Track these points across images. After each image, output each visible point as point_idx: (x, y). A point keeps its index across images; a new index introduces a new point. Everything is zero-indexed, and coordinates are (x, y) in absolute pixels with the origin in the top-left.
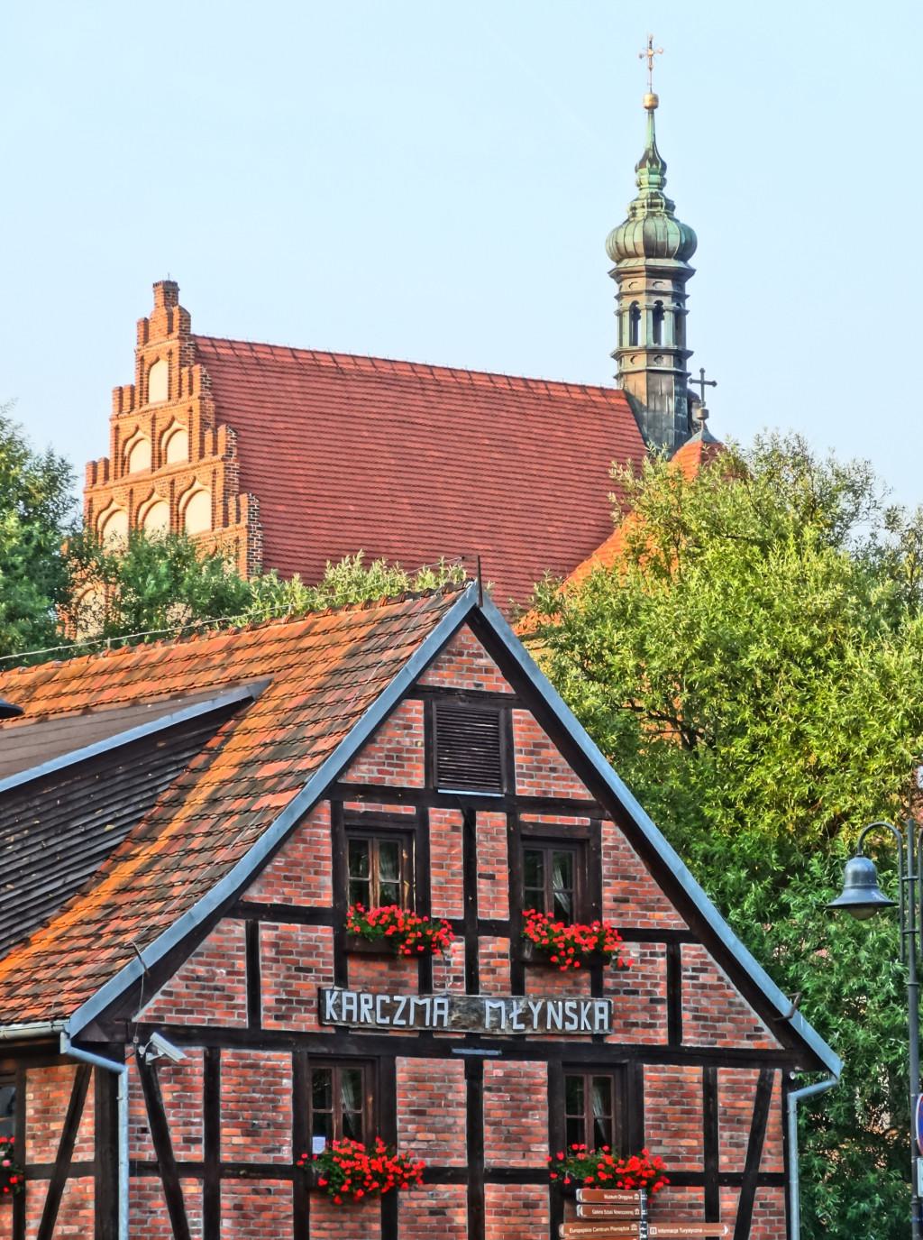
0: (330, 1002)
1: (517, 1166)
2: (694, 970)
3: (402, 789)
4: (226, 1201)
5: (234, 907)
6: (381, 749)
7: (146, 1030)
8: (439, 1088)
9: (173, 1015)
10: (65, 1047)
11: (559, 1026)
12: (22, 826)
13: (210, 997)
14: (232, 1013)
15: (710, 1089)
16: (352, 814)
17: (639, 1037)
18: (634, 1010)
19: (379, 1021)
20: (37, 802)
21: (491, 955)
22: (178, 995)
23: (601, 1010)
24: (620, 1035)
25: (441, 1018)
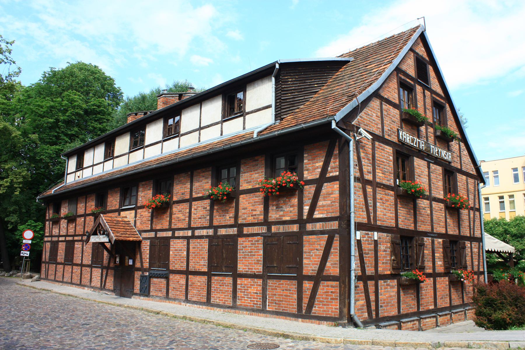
0: (401, 134)
4: (378, 196)
5: (376, 94)
10: (334, 126)
12: (293, 77)
13: (372, 123)
22: (364, 119)
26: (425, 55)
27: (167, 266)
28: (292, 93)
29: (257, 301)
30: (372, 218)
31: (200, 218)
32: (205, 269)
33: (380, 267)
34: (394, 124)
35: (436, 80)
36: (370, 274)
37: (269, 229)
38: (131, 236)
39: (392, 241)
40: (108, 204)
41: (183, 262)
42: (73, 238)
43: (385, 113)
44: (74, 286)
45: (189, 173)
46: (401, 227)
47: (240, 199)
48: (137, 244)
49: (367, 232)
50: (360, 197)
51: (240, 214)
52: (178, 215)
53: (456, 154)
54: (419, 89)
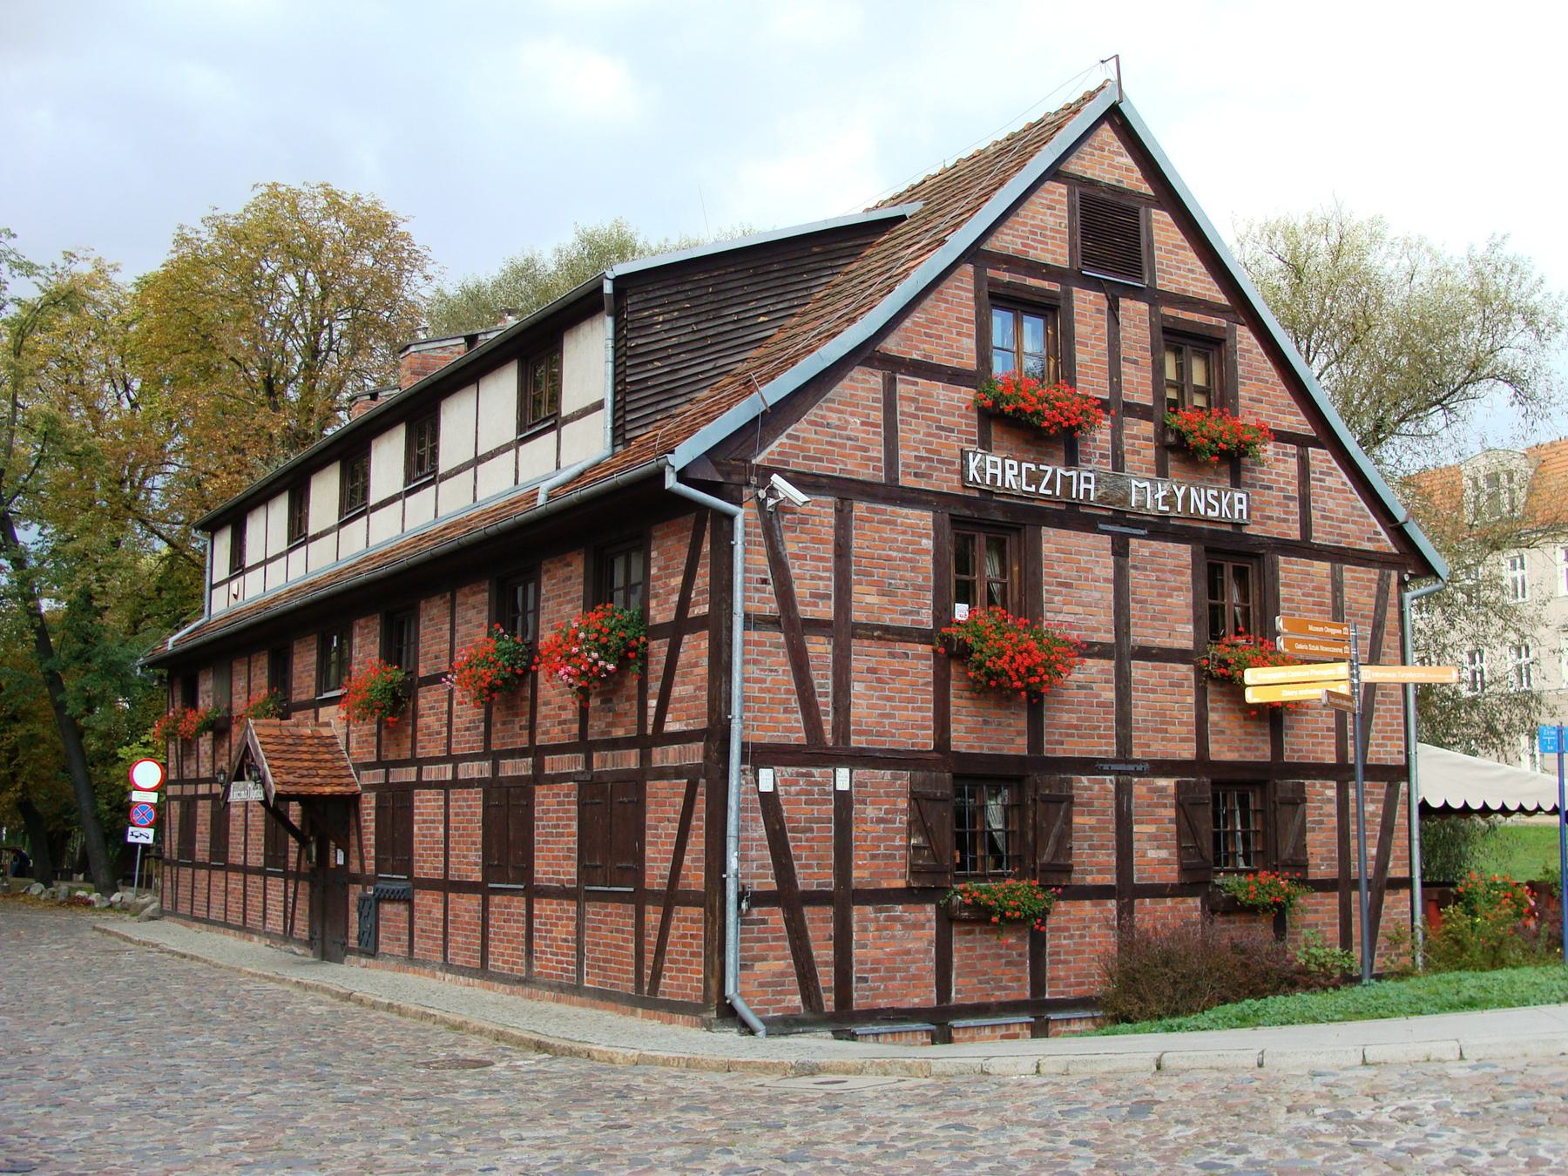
0: (972, 465)
1: (1163, 645)
2: (1321, 473)
3: (1046, 266)
4: (858, 663)
5: (865, 354)
6: (1025, 224)
7: (766, 472)
8: (1086, 562)
9: (800, 460)
10: (671, 482)
11: (1202, 513)
14: (867, 466)
15: (1337, 587)
16: (993, 283)
17: (1274, 530)
18: (1269, 503)
19: (1025, 488)
20: (687, 287)
21: (1135, 437)
23: (1240, 501)
24: (1257, 527)
25: (1087, 491)
26: (1132, 178)
27: (406, 866)
28: (669, 357)
29: (567, 963)
30: (828, 728)
31: (467, 729)
32: (477, 876)
33: (859, 867)
34: (947, 438)
35: (1191, 257)
36: (815, 888)
37: (588, 762)
38: (329, 780)
39: (912, 792)
41: (436, 856)
42: (387, 775)
43: (902, 407)
44: (231, 931)
45: (448, 595)
46: (963, 750)
48: (351, 802)
49: (804, 770)
50: (776, 671)
51: (539, 720)
53: (1281, 490)
54: (1087, 305)
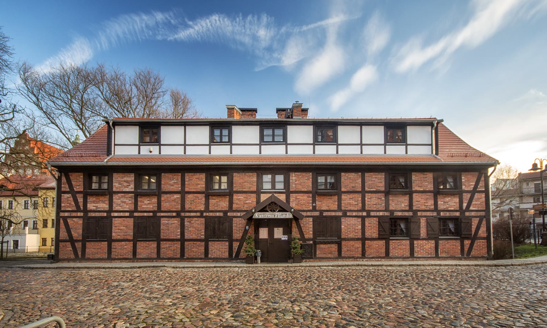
40: (234, 185)
47: (413, 195)
51: (414, 204)
52: (349, 202)
